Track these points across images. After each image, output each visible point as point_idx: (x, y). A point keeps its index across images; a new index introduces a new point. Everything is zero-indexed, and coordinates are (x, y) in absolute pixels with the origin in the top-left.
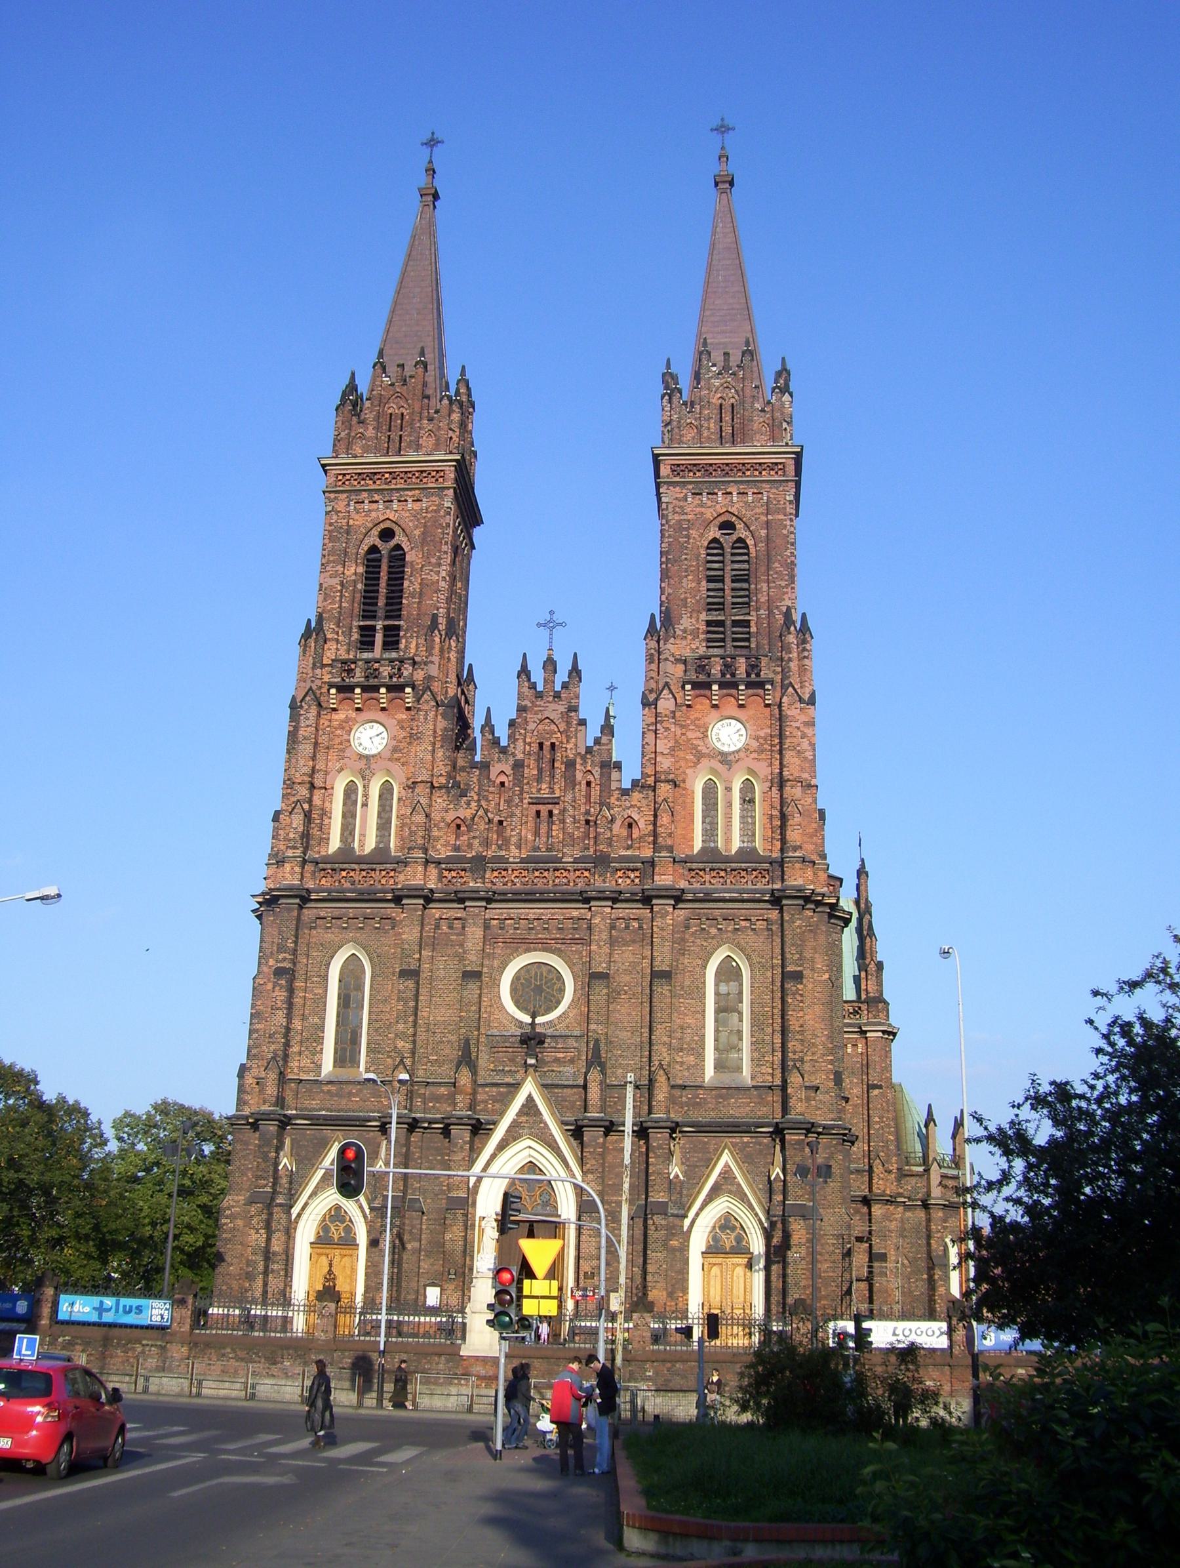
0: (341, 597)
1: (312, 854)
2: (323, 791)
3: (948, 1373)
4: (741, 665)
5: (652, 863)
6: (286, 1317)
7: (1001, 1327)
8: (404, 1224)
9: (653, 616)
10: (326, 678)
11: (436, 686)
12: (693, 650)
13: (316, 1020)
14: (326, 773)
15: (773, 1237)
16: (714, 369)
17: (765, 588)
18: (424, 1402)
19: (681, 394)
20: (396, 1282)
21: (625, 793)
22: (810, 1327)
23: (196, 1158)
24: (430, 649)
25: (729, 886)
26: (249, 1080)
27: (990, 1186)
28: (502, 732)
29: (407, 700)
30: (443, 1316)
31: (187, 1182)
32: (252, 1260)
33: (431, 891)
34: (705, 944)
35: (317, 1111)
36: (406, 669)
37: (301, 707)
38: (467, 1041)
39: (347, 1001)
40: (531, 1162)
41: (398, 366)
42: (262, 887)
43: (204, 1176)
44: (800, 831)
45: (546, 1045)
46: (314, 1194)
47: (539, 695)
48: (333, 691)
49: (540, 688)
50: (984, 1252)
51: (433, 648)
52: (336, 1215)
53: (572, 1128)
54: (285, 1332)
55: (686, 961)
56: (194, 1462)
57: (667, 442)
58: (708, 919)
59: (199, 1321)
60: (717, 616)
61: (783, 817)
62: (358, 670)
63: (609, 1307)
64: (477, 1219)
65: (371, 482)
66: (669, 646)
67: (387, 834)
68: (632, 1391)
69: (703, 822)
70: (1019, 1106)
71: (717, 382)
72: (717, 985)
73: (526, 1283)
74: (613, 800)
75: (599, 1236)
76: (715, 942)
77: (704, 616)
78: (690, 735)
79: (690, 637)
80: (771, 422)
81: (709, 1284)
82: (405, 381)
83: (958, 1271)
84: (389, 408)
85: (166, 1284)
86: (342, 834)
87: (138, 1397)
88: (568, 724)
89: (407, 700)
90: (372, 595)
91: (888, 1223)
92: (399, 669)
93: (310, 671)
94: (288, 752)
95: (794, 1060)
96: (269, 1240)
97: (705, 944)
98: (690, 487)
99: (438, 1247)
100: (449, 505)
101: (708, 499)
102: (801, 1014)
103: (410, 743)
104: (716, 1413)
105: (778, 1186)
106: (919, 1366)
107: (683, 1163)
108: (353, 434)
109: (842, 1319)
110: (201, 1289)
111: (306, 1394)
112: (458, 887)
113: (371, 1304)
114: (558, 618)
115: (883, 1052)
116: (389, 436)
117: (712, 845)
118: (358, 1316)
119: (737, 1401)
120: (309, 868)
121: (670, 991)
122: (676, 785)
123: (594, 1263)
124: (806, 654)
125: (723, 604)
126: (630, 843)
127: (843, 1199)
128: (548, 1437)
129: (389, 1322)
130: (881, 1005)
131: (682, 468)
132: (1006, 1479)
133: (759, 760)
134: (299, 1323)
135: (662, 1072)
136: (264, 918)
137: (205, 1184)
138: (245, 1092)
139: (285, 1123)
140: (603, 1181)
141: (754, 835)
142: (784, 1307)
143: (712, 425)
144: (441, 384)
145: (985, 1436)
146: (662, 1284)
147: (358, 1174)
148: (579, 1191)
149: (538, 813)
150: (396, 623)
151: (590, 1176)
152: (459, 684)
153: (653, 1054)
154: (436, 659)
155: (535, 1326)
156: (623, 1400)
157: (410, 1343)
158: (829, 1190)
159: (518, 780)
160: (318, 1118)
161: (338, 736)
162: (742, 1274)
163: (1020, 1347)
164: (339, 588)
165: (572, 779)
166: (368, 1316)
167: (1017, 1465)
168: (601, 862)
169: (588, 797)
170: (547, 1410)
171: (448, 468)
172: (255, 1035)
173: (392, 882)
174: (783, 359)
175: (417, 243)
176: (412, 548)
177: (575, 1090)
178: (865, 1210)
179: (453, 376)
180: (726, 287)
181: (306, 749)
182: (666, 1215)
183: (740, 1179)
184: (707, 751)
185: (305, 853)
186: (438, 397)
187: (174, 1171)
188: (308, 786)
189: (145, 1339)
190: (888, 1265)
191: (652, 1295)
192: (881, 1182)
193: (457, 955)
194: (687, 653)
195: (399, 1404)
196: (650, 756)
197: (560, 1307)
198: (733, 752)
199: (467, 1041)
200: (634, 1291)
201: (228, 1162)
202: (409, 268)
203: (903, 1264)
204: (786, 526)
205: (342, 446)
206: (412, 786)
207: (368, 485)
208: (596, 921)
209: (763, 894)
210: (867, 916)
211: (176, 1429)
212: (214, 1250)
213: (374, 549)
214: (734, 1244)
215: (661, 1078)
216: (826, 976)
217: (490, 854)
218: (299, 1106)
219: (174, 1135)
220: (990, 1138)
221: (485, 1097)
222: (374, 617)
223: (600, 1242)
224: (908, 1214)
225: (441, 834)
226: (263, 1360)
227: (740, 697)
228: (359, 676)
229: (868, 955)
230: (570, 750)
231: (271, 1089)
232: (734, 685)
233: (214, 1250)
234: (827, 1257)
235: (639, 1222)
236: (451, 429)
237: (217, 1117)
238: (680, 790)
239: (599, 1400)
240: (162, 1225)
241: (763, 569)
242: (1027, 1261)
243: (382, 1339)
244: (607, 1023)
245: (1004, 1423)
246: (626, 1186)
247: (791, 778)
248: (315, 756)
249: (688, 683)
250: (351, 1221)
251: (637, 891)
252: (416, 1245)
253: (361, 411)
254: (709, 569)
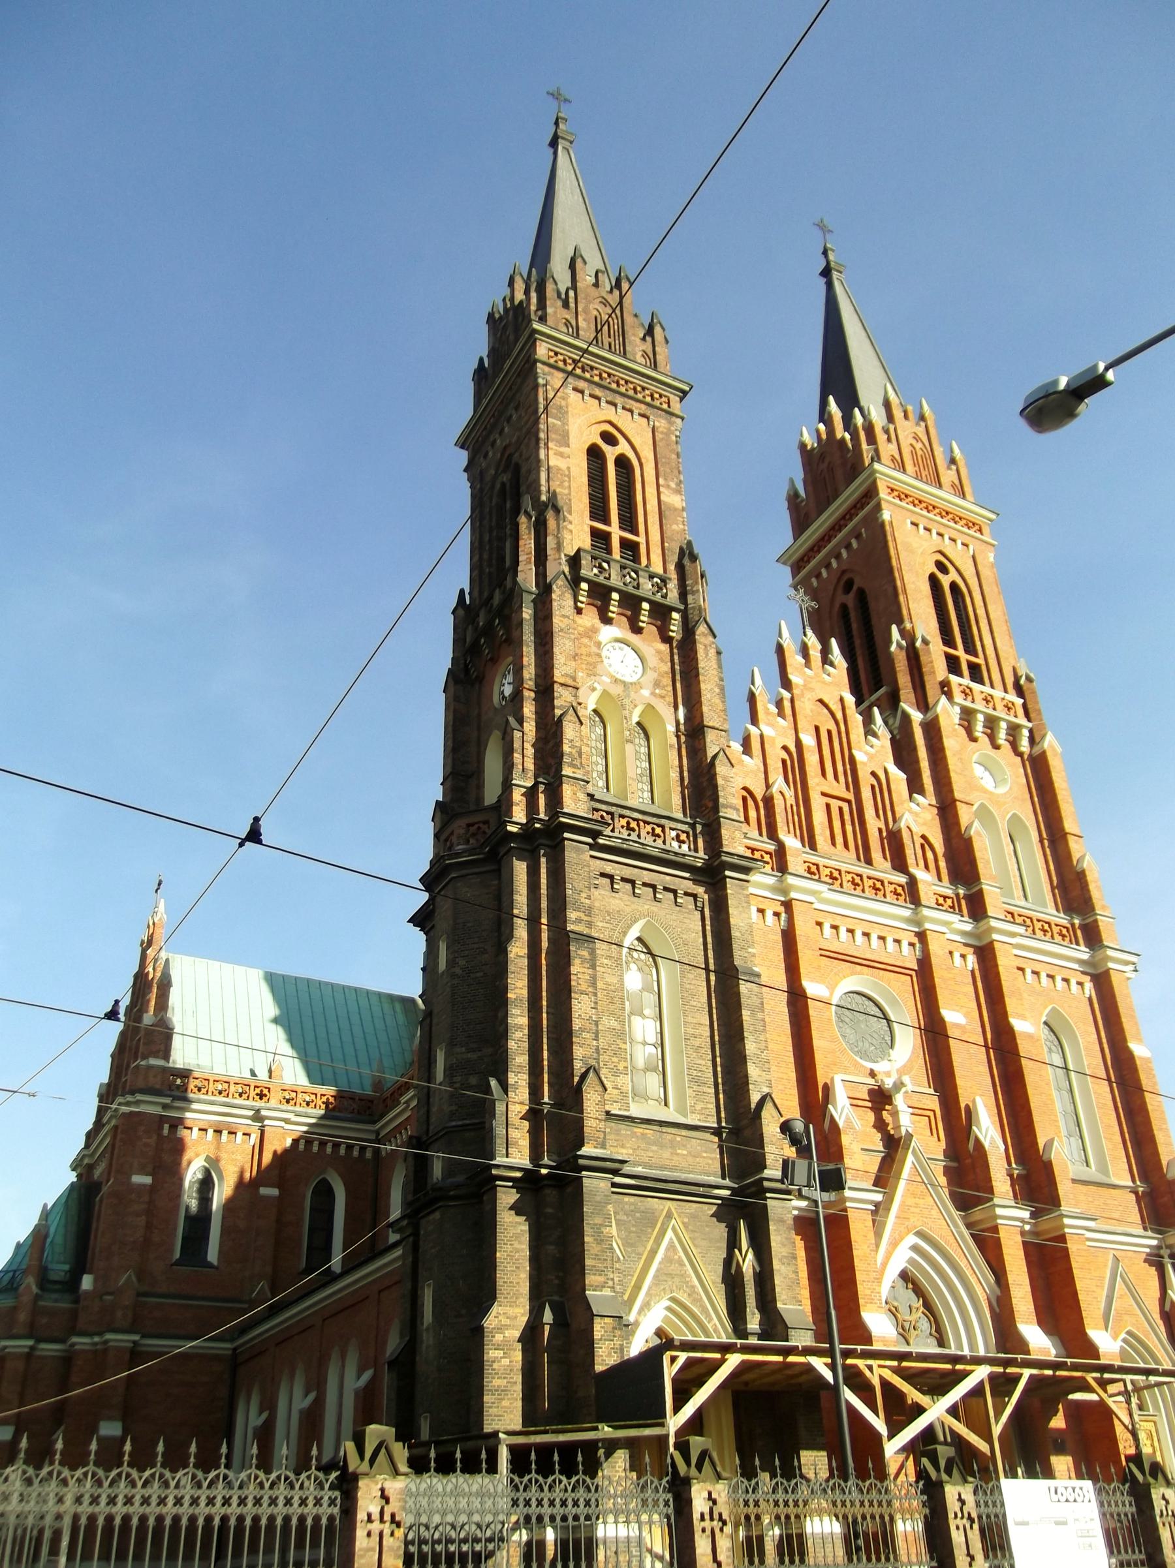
13: (614, 1024)
161: (586, 646)
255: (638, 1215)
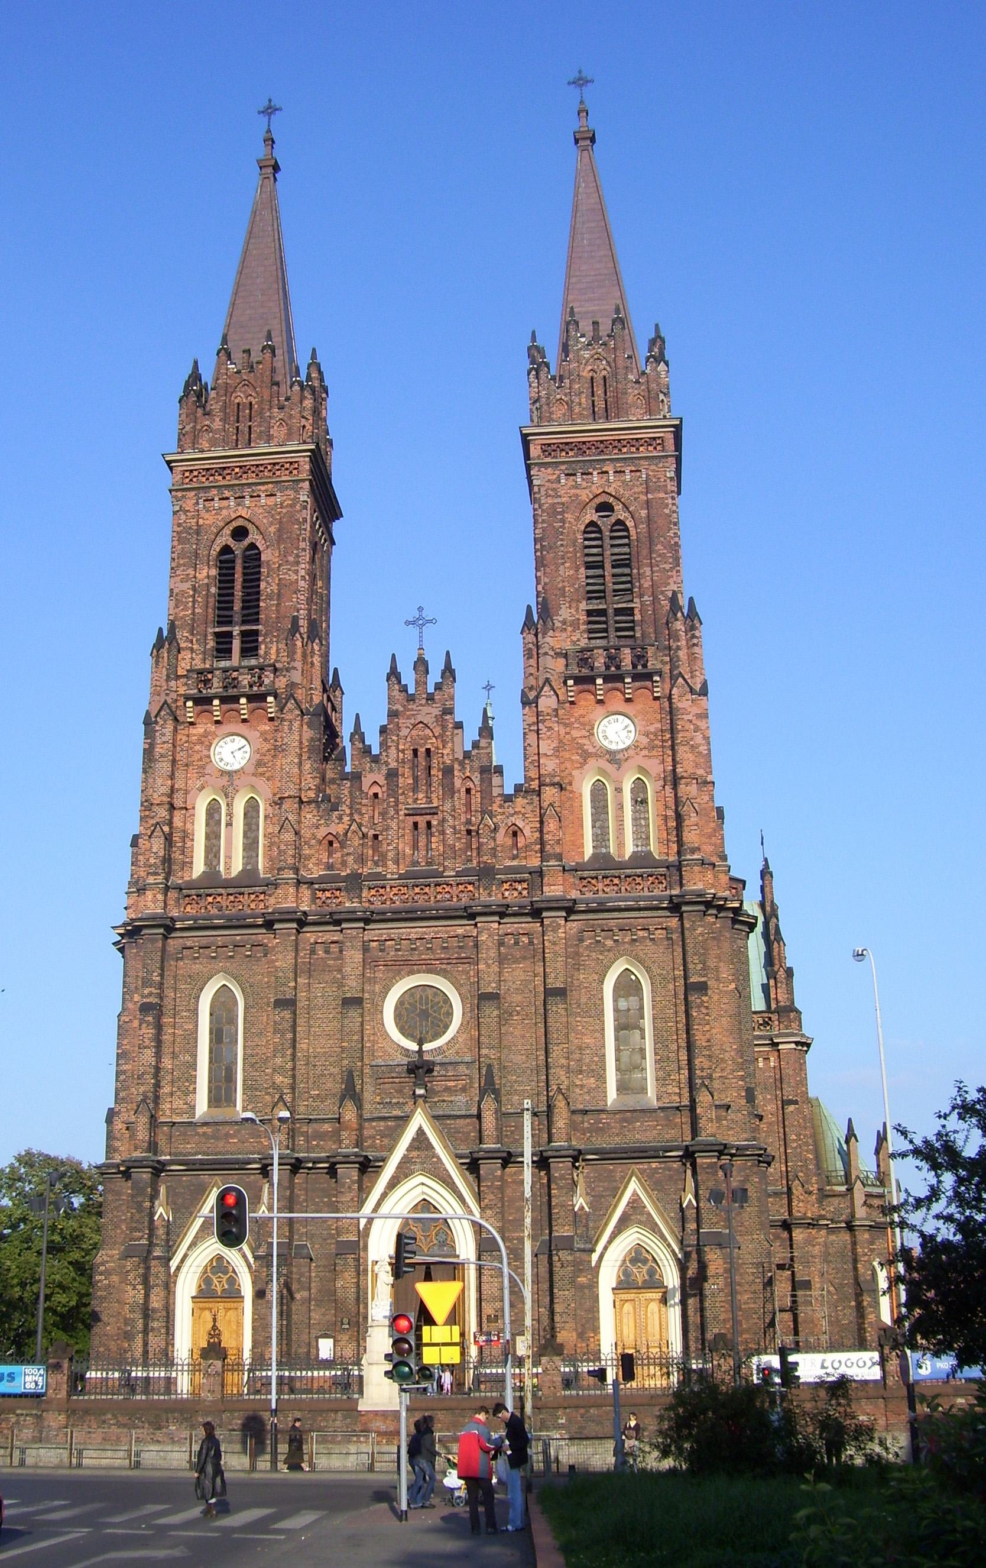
0: (194, 602)
1: (175, 880)
2: (184, 812)
3: (883, 1406)
4: (627, 657)
5: (540, 873)
6: (169, 1378)
7: (937, 1354)
8: (291, 1273)
9: (529, 608)
10: (182, 690)
11: (300, 694)
12: (574, 643)
13: (188, 1058)
14: (186, 792)
15: (688, 1268)
16: (583, 340)
17: (648, 573)
18: (321, 1462)
19: (549, 369)
20: (285, 1335)
21: (508, 799)
22: (732, 1363)
23: (65, 1212)
24: (291, 654)
25: (623, 894)
26: (119, 1125)
27: (919, 1203)
28: (373, 740)
29: (270, 710)
30: (338, 1369)
31: (57, 1238)
32: (130, 1319)
33: (305, 913)
34: (601, 957)
35: (192, 1155)
36: (266, 676)
37: (156, 722)
38: (350, 1074)
39: (218, 1036)
40: (424, 1200)
41: (244, 352)
42: (123, 917)
43: (74, 1231)
44: (698, 832)
45: (435, 1073)
46: (193, 1245)
47: (411, 698)
48: (190, 704)
49: (411, 690)
50: (915, 1275)
51: (294, 653)
52: (219, 1265)
53: (467, 1161)
54: (169, 1394)
55: (582, 976)
56: (78, 1538)
57: (536, 420)
58: (603, 931)
59: (76, 1387)
60: (598, 604)
61: (679, 818)
62: (215, 680)
63: (515, 1351)
64: (370, 1263)
65: (220, 478)
66: (548, 639)
67: (254, 855)
68: (544, 1441)
69: (593, 827)
70: (945, 1116)
71: (586, 354)
72: (615, 1001)
73: (426, 1329)
74: (495, 807)
75: (502, 1275)
76: (611, 955)
77: (584, 606)
78: (575, 733)
79: (570, 629)
80: (646, 394)
81: (621, 1321)
82: (252, 367)
83: (888, 1296)
84: (236, 398)
85: (39, 1348)
86: (206, 857)
87: (15, 1470)
88: (444, 727)
89: (270, 710)
90: (227, 598)
91: (811, 1248)
92: (260, 677)
93: (164, 684)
94: (145, 771)
95: (702, 1078)
96: (147, 1296)
97: (601, 957)
98: (563, 467)
99: (330, 1296)
100: (305, 498)
101: (583, 480)
102: (707, 1028)
103: (274, 756)
104: (635, 1460)
105: (691, 1214)
106: (850, 1400)
107: (587, 1194)
108: (198, 427)
109: (766, 1354)
110: (77, 1352)
111: (194, 1460)
112: (334, 908)
113: (260, 1360)
114: (427, 614)
115: (797, 1065)
116: (238, 427)
117: (604, 850)
118: (246, 1373)
119: (657, 1447)
120: (173, 894)
121: (566, 1009)
122: (562, 789)
123: (498, 1305)
124: (695, 641)
125: (604, 591)
126: (515, 852)
127: (761, 1224)
128: (457, 1494)
129: (280, 1379)
130: (792, 1015)
131: (554, 447)
132: (950, 1517)
133: (650, 757)
134: (184, 1384)
135: (560, 1097)
136: (127, 951)
137: (76, 1239)
138: (115, 1138)
139: (158, 1169)
140: (503, 1216)
141: (648, 838)
142: (703, 1344)
143: (583, 400)
144: (291, 369)
145: (925, 1472)
146: (571, 1325)
147: (240, 1221)
148: (478, 1228)
149: (416, 825)
150: (254, 628)
151: (489, 1212)
152: (325, 690)
153: (550, 1078)
154: (298, 664)
155: (436, 1376)
156: (535, 1451)
157: (305, 1400)
158: (746, 1216)
159: (393, 790)
160: (194, 1162)
161: (197, 752)
162: (656, 1309)
163: (958, 1375)
164: (191, 593)
165: (450, 787)
166: (257, 1373)
167: (961, 1502)
168: (486, 874)
169: (468, 805)
170: (453, 1465)
171: (302, 459)
172: (122, 1077)
173: (262, 906)
174: (657, 326)
175: (258, 218)
176: (267, 547)
177: (468, 1120)
178: (785, 1235)
179: (303, 360)
180: (591, 252)
181: (163, 767)
182: (572, 1249)
183: (650, 1208)
184: (594, 750)
185: (167, 879)
186: (289, 383)
187: (42, 1227)
188: (167, 807)
189: (19, 1408)
190: (812, 1293)
191: (562, 1337)
192: (801, 1204)
193: (335, 981)
194: (568, 646)
195: (295, 1467)
196: (533, 759)
197: (463, 1354)
198: (622, 750)
199: (350, 1074)
200: (542, 1333)
201: (99, 1214)
202: (251, 247)
203: (828, 1291)
204: (667, 505)
205: (188, 440)
206: (279, 802)
207: (217, 481)
208: (483, 937)
209: (661, 901)
210: (774, 920)
211: (56, 1503)
212: (89, 1309)
213: (226, 550)
214: (647, 1277)
215: (560, 1104)
216: (733, 986)
217: (366, 871)
218: (173, 1150)
219: (41, 1188)
220: (916, 1152)
221: (372, 1132)
222: (230, 623)
223: (502, 1282)
224: (832, 1237)
225: (313, 852)
226: (147, 1425)
227: (627, 691)
228: (217, 686)
229: (776, 962)
230: (446, 755)
231: (142, 1134)
232: (620, 678)
233: (89, 1309)
234: (747, 1287)
235: (544, 1258)
236: (303, 417)
237: (85, 1166)
238: (567, 793)
239: (509, 1452)
240: (32, 1284)
241: (645, 552)
242: (962, 1282)
243: (274, 1397)
244: (500, 1047)
245: (945, 1457)
246: (528, 1221)
247: (685, 775)
248: (173, 774)
249: (570, 678)
250: (234, 1271)
251: (526, 904)
252: (305, 1294)
253: (206, 402)
254: (587, 555)
255: (192, 1188)
